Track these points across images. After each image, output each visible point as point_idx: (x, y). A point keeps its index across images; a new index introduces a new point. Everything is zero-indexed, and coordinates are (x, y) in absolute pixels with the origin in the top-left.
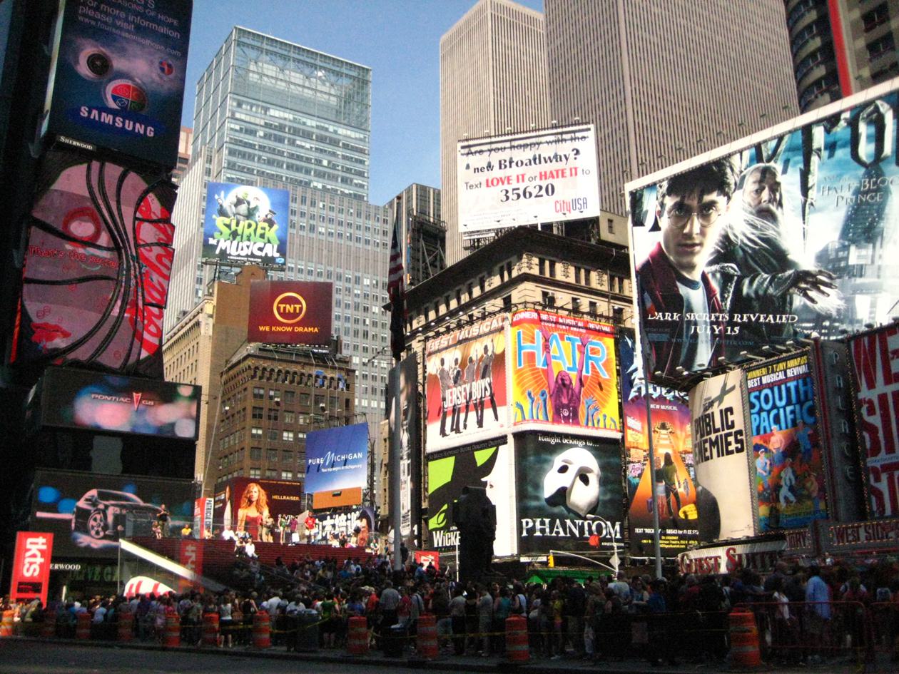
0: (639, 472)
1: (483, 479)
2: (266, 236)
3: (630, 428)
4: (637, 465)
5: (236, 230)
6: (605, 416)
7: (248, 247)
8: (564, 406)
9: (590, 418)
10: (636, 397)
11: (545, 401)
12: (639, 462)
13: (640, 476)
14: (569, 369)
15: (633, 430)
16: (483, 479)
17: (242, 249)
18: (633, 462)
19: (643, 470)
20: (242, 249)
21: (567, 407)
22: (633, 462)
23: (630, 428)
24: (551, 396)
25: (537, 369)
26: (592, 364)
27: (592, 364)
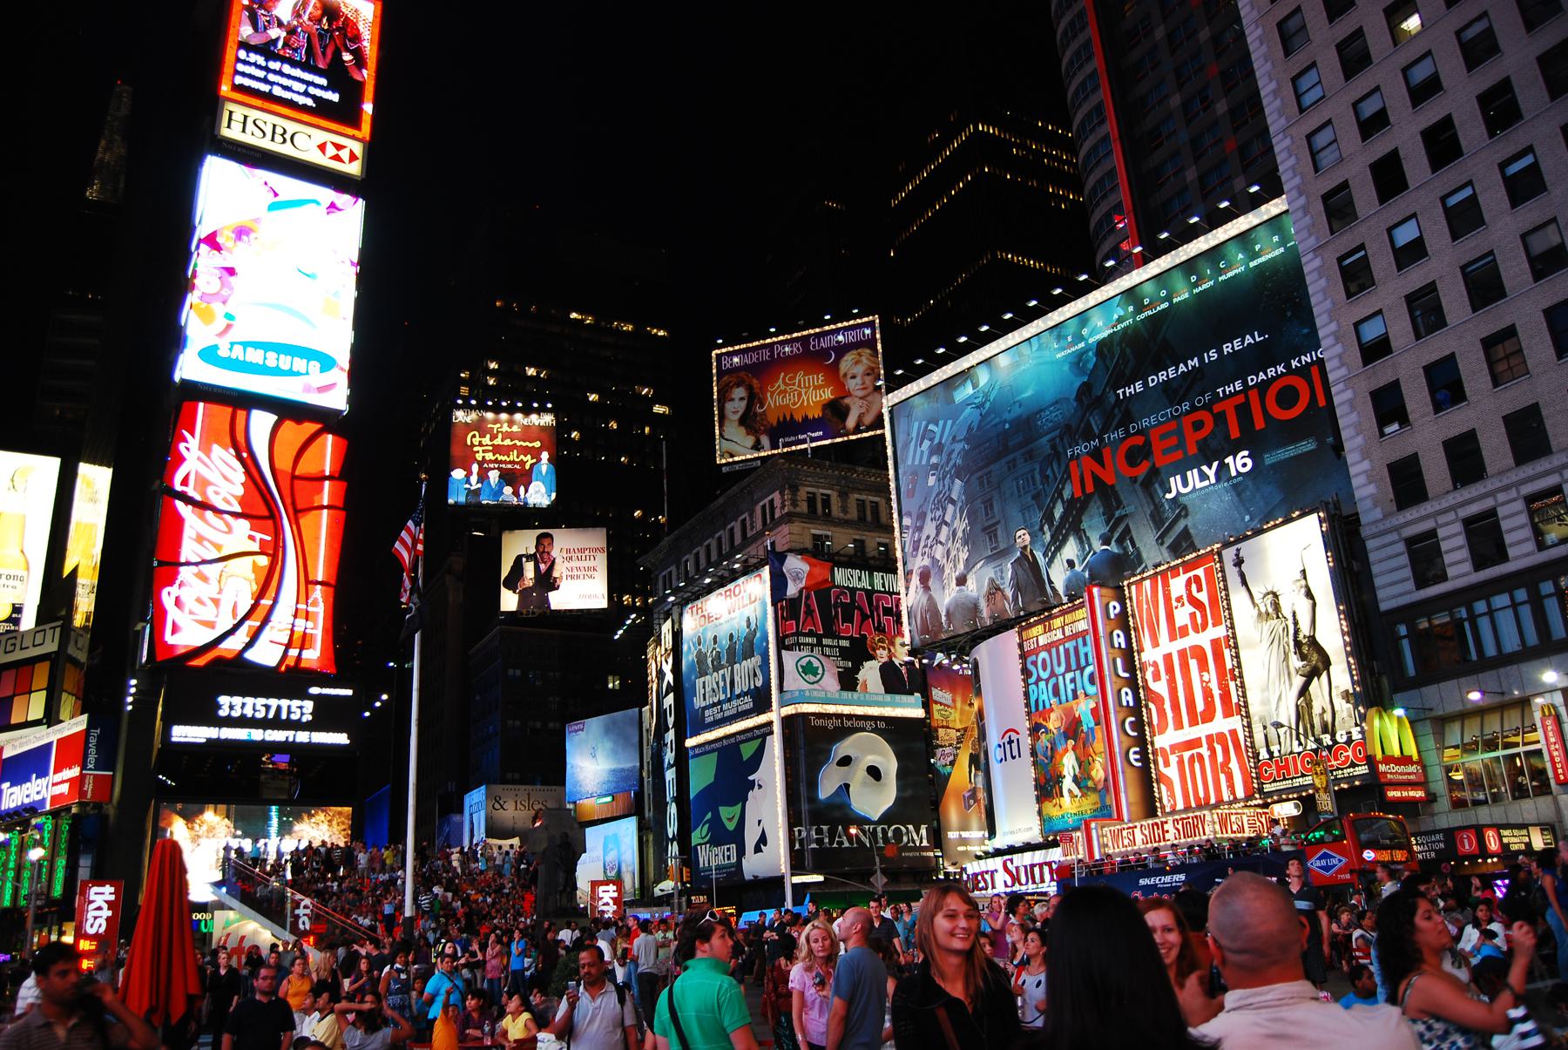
4: (948, 750)
13: (952, 763)
19: (956, 756)
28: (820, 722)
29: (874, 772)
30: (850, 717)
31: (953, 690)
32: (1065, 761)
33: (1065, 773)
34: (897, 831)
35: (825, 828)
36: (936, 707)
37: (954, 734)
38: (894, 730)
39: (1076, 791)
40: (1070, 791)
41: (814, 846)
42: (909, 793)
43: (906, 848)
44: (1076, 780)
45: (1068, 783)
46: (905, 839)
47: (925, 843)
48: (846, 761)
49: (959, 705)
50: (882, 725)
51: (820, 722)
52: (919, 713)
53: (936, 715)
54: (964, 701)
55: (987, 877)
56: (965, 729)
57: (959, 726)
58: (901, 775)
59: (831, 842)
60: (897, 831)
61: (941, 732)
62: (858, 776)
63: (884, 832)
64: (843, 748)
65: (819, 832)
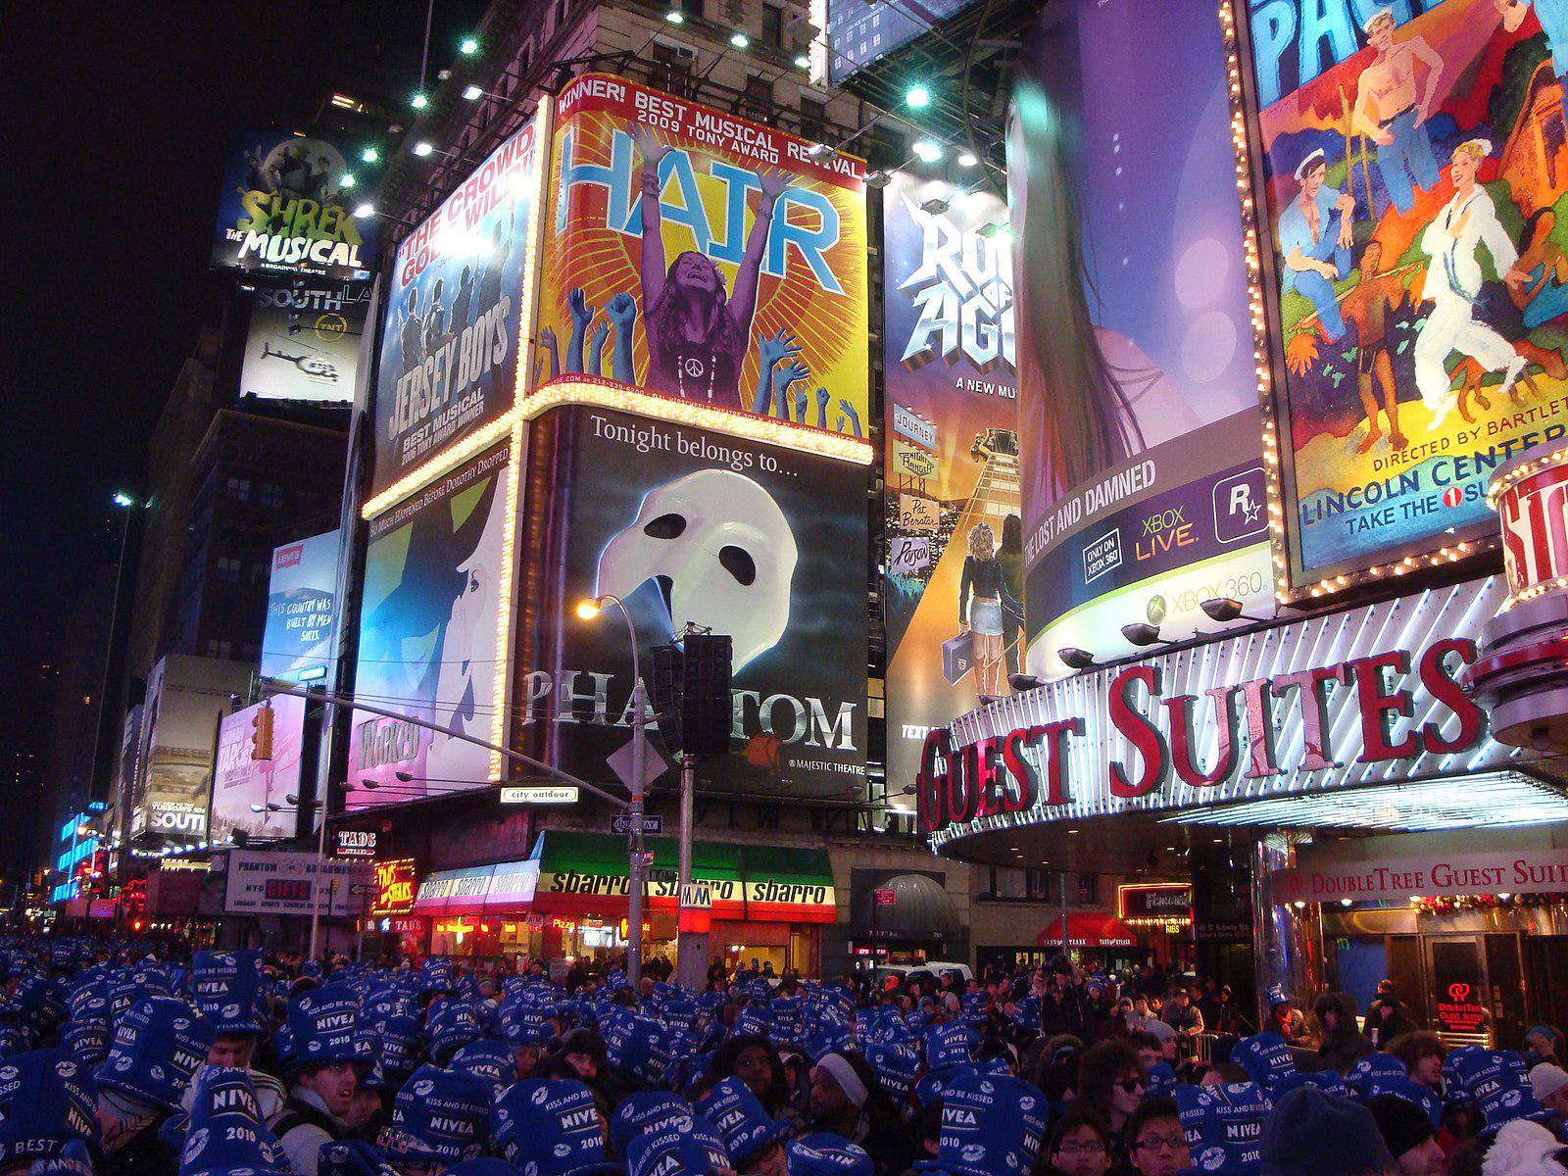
0: (924, 562)
1: (461, 569)
2: (338, 228)
3: (901, 437)
4: (918, 544)
5: (281, 216)
6: (824, 395)
7: (301, 247)
8: (689, 350)
9: (776, 393)
10: (924, 354)
11: (627, 326)
12: (925, 533)
13: (926, 573)
14: (714, 249)
15: (912, 443)
16: (461, 569)
17: (290, 252)
18: (904, 533)
19: (935, 558)
20: (290, 252)
21: (702, 352)
22: (904, 533)
23: (901, 437)
24: (646, 316)
25: (614, 234)
26: (792, 248)
27: (792, 248)
28: (618, 433)
29: (739, 563)
30: (693, 432)
31: (940, 416)
32: (1434, 240)
33: (1434, 286)
34: (782, 708)
35: (601, 679)
36: (899, 448)
37: (935, 512)
38: (800, 482)
39: (1493, 350)
40: (1458, 366)
41: (567, 717)
42: (819, 625)
43: (800, 750)
44: (1498, 306)
45: (1449, 328)
46: (800, 729)
47: (846, 743)
48: (670, 526)
49: (950, 450)
50: (770, 464)
51: (618, 433)
52: (864, 455)
53: (898, 465)
54: (962, 445)
55: (1037, 757)
56: (961, 505)
57: (946, 495)
58: (806, 581)
59: (612, 716)
60: (782, 708)
61: (907, 502)
62: (693, 566)
63: (750, 706)
64: (668, 497)
65: (584, 685)
